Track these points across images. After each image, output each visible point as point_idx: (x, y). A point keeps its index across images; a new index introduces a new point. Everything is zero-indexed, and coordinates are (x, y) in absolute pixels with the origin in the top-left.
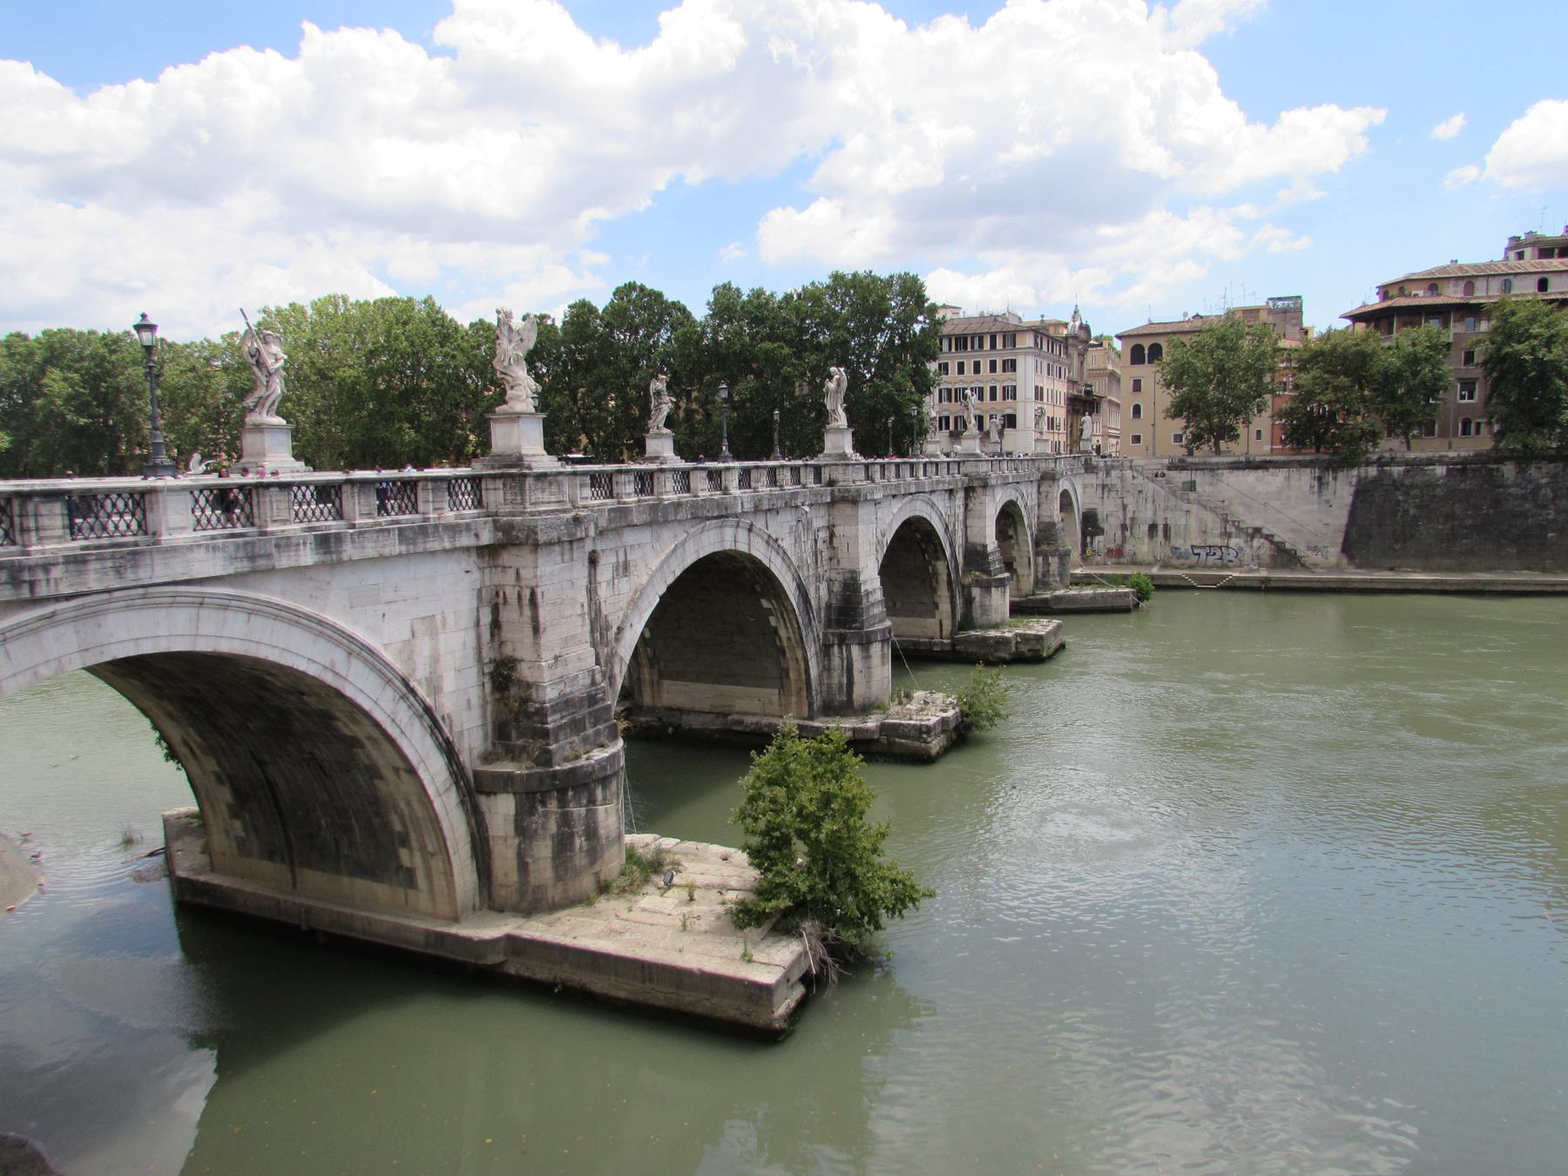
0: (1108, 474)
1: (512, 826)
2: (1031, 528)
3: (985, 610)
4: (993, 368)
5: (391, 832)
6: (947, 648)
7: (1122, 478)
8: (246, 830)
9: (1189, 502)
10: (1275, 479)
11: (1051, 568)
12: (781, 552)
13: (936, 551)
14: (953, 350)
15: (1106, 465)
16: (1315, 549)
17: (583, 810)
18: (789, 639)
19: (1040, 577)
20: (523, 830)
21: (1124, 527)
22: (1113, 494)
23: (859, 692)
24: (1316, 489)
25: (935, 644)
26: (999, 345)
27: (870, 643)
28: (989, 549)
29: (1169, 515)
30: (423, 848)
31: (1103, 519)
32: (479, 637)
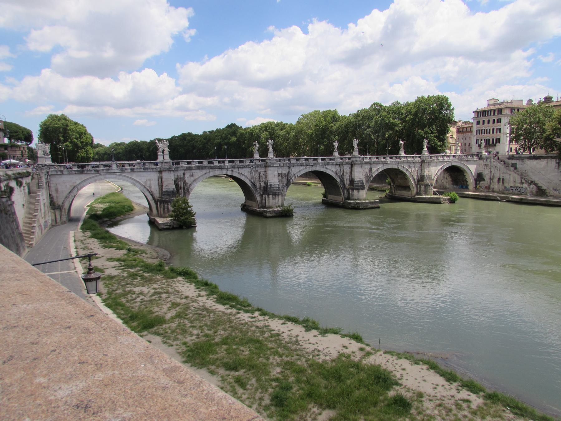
0: (487, 160)
3: (353, 196)
4: (494, 122)
7: (490, 162)
9: (510, 171)
10: (543, 163)
16: (556, 190)
20: (160, 207)
21: (490, 179)
22: (488, 167)
23: (267, 204)
24: (557, 167)
26: (496, 114)
27: (268, 195)
28: (355, 180)
29: (504, 175)
32: (159, 182)
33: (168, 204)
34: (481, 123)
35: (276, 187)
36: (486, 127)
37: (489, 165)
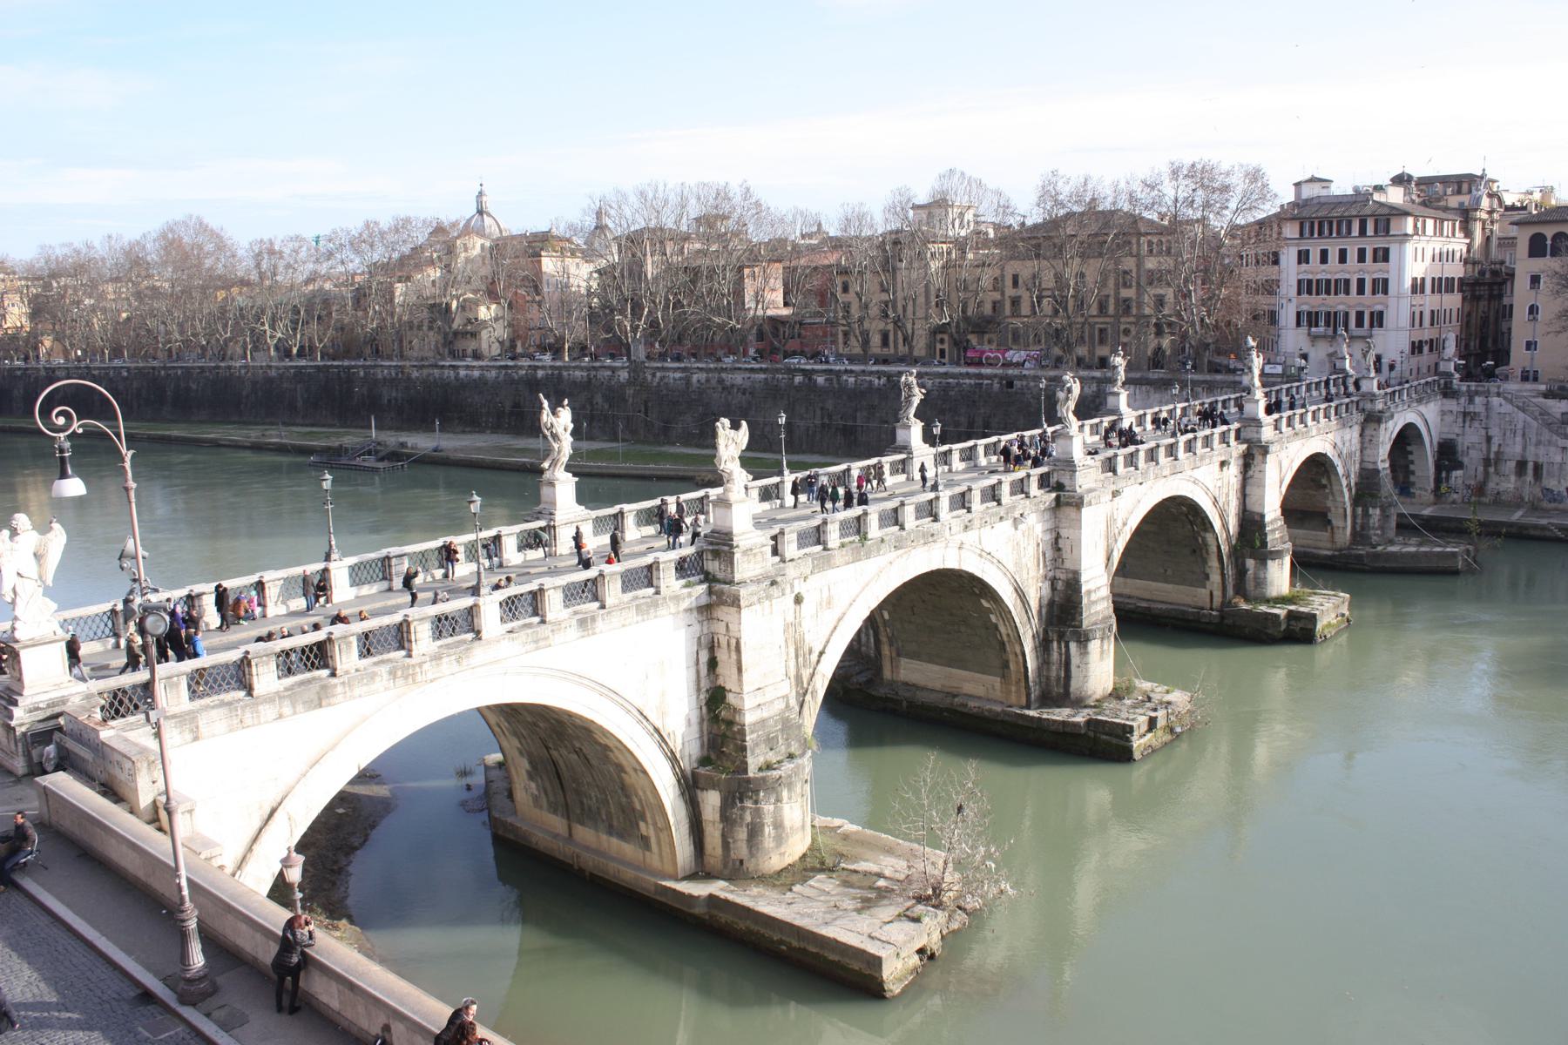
0: (1471, 401)
1: (718, 815)
2: (1348, 477)
3: (1261, 582)
5: (634, 810)
6: (1216, 621)
8: (538, 790)
11: (1371, 521)
12: (995, 561)
13: (1204, 524)
14: (1316, 236)
15: (1469, 391)
17: (772, 807)
18: (1008, 635)
19: (1358, 529)
21: (1487, 462)
22: (1476, 424)
25: (1204, 615)
26: (1370, 230)
28: (1267, 519)
29: (1542, 450)
30: (655, 824)
31: (1463, 451)
32: (698, 672)
33: (779, 800)
34: (1315, 256)
35: (1103, 599)
36: (1333, 270)
37: (1483, 416)
